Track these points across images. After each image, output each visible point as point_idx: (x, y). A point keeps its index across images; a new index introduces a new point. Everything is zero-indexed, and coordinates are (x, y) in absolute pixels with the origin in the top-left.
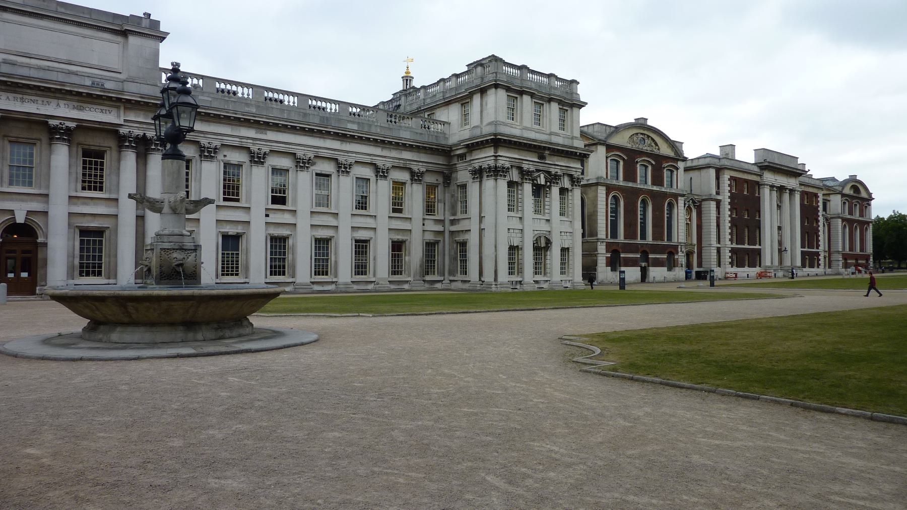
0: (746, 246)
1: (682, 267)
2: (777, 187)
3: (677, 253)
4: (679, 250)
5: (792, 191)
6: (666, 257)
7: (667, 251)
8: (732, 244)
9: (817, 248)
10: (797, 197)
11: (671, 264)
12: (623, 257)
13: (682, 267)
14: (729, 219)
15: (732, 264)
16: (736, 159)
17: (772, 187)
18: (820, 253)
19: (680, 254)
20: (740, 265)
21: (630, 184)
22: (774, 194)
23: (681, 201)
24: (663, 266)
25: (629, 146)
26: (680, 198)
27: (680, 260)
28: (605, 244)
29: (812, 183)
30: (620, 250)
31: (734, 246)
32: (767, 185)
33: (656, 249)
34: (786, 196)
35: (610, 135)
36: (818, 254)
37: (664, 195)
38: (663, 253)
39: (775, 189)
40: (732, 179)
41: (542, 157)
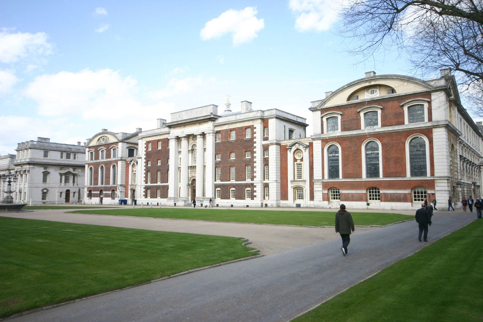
0: (159, 184)
1: (119, 197)
2: (185, 137)
3: (117, 190)
4: (118, 188)
5: (203, 135)
6: (111, 192)
7: (112, 190)
8: (146, 183)
9: (253, 178)
10: (210, 139)
11: (113, 196)
12: (93, 193)
13: (119, 197)
14: (145, 168)
15: (146, 196)
16: (218, 115)
17: (178, 139)
18: (255, 185)
19: (118, 190)
20: (154, 196)
21: (108, 160)
22: (184, 142)
23: (120, 163)
24: (109, 197)
25: (97, 144)
26: (119, 162)
27: (118, 194)
28: (87, 188)
29: (243, 118)
30: (92, 190)
31: (149, 184)
32: (172, 139)
33: (107, 189)
34: (199, 140)
35: (89, 143)
36: (252, 186)
37: (111, 162)
38: (109, 191)
39: (182, 139)
40: (148, 143)
41: (22, 167)
